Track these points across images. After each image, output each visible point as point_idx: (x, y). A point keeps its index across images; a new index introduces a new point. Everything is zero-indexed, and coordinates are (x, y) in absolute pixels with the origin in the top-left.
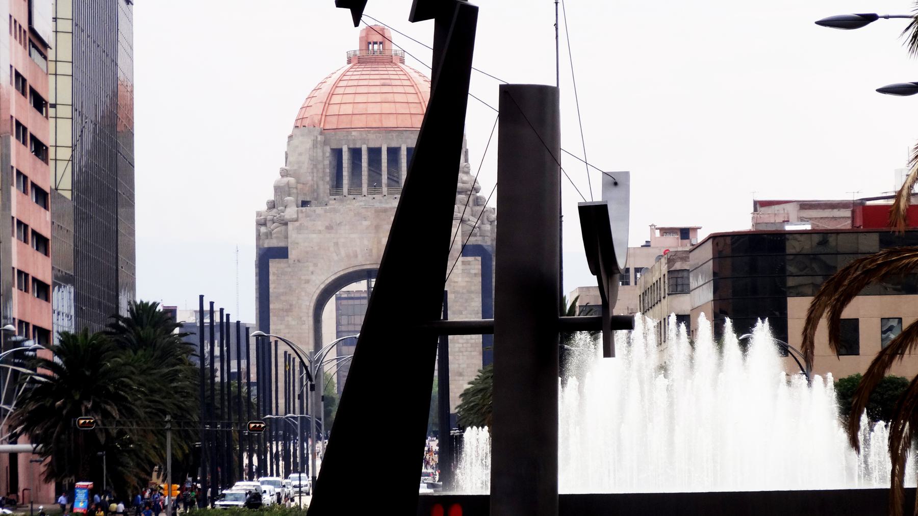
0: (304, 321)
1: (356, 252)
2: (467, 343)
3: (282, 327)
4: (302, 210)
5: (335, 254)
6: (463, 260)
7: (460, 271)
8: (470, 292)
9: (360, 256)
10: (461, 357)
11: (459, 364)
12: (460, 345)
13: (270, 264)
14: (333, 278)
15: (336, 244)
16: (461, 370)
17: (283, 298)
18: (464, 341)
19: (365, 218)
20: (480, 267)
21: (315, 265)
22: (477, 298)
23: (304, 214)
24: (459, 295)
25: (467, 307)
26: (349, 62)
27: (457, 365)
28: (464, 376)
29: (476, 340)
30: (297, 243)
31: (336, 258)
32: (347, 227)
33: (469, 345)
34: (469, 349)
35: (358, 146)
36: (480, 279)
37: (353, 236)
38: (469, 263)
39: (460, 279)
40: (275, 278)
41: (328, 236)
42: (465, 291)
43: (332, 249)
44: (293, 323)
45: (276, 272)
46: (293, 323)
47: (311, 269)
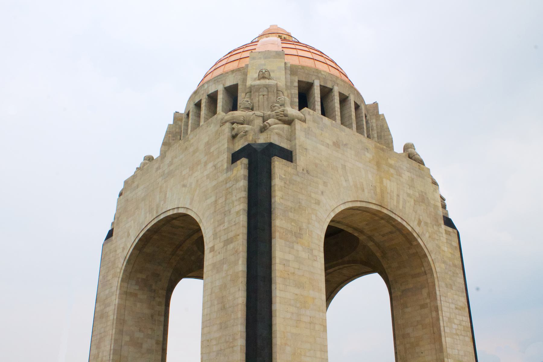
0: (316, 256)
2: (460, 325)
5: (342, 178)
7: (445, 241)
9: (366, 191)
14: (343, 208)
15: (344, 167)
17: (291, 215)
21: (325, 184)
30: (306, 149)
31: (344, 184)
35: (329, 85)
39: (446, 249)
40: (282, 184)
44: (304, 255)
45: (284, 177)
46: (304, 255)
47: (321, 187)
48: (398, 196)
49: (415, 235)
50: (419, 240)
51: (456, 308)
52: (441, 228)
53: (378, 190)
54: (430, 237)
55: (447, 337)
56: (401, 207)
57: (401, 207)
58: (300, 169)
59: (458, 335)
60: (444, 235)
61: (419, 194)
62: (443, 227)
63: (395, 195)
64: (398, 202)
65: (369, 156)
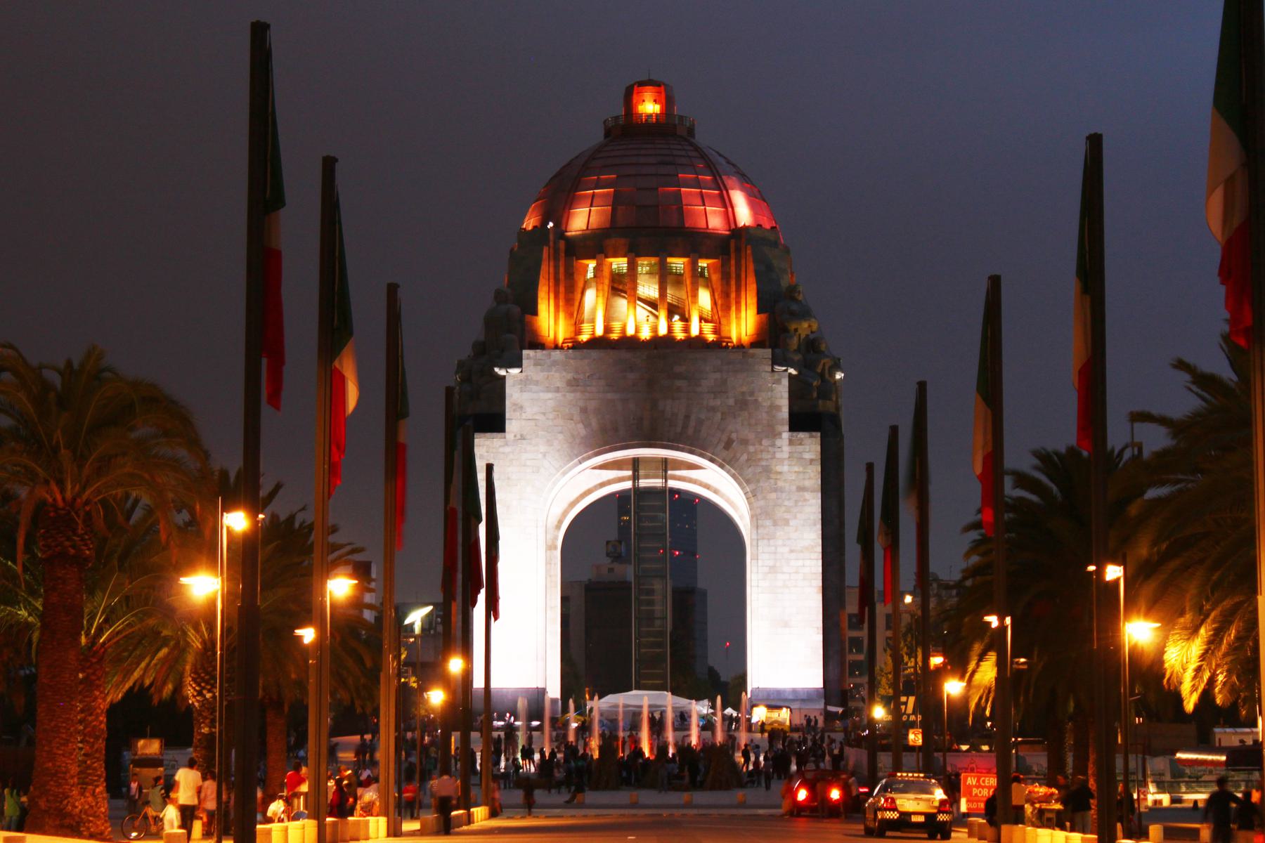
2: (797, 572)
4: (528, 355)
7: (786, 455)
13: (476, 441)
20: (819, 448)
22: (814, 498)
23: (532, 362)
24: (784, 495)
26: (608, 133)
30: (521, 407)
39: (785, 468)
42: (794, 488)
45: (486, 454)
51: (792, 551)
52: (781, 438)
54: (748, 460)
57: (690, 431)
60: (786, 448)
61: (736, 402)
62: (786, 435)
64: (685, 427)
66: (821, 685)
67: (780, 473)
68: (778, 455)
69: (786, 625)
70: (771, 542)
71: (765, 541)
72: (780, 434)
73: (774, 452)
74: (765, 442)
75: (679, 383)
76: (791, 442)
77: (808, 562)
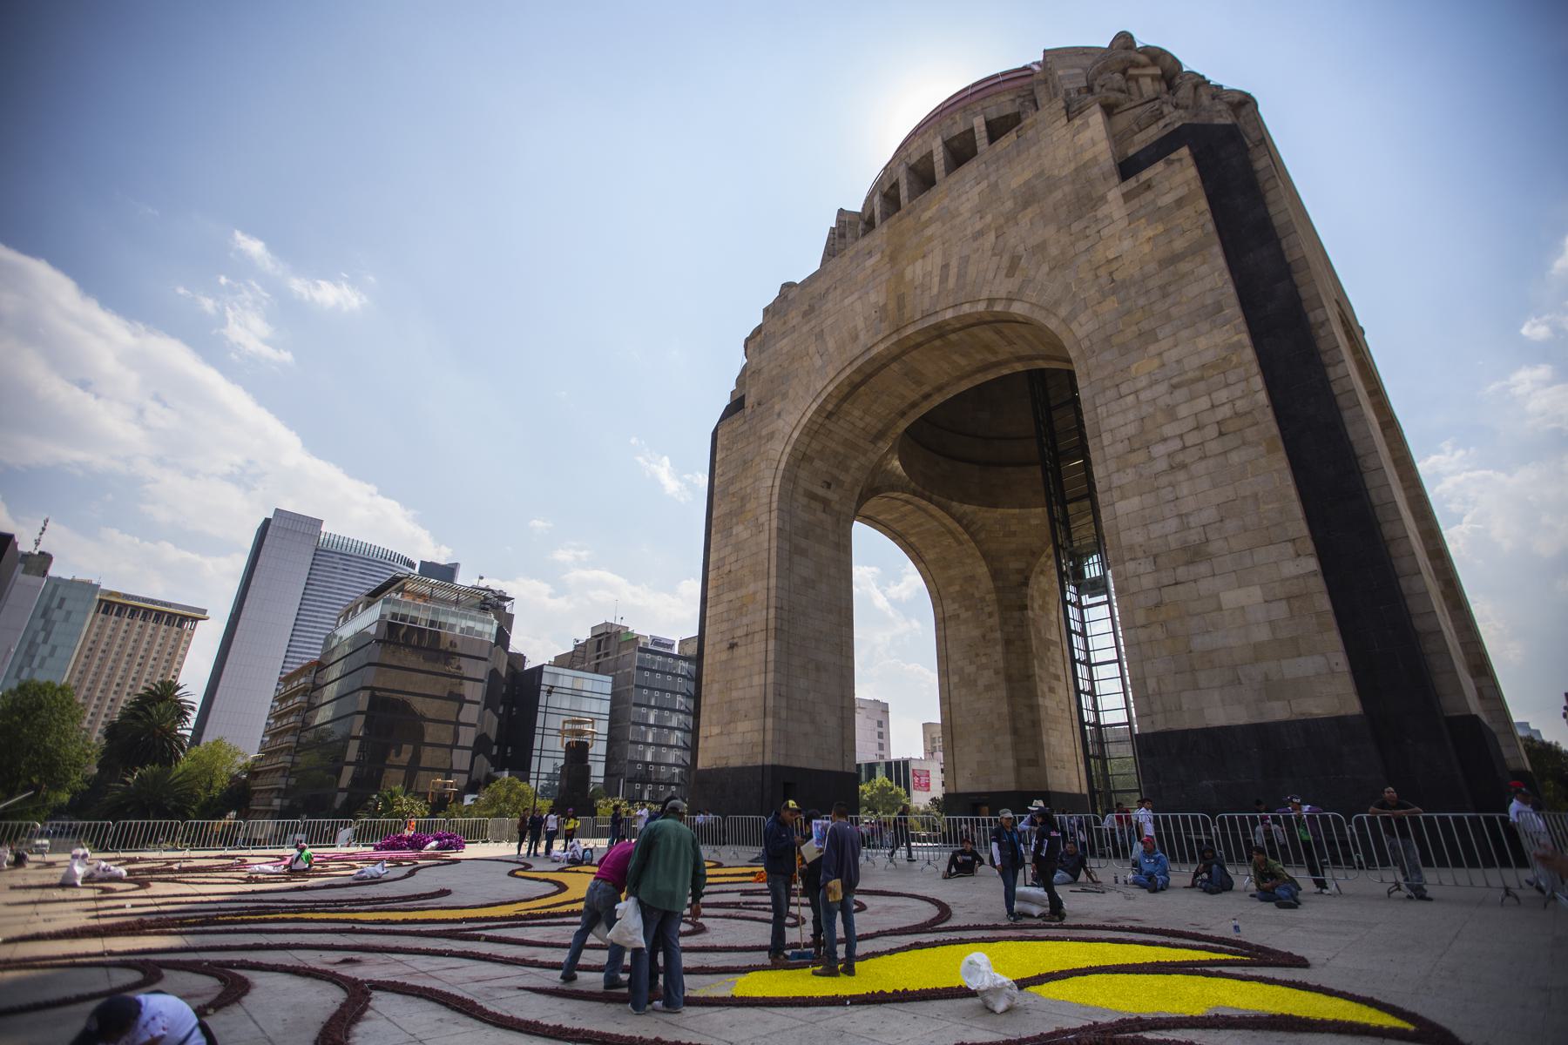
1: (856, 329)
2: (1199, 428)
3: (729, 549)
6: (1125, 190)
8: (1175, 259)
9: (863, 337)
10: (1185, 489)
11: (1180, 516)
12: (1177, 444)
16: (1194, 537)
18: (1191, 423)
19: (870, 254)
20: (1192, 172)
21: (784, 396)
22: (1204, 263)
24: (1133, 291)
25: (1174, 311)
27: (1173, 524)
28: (1209, 557)
29: (1239, 403)
31: (818, 362)
32: (839, 291)
33: (1212, 431)
34: (1214, 447)
36: (1203, 204)
37: (847, 302)
38: (1148, 186)
41: (805, 329)
42: (1152, 267)
43: (812, 349)
46: (745, 535)
47: (777, 408)
48: (946, 266)
49: (998, 308)
50: (1018, 309)
51: (1174, 387)
52: (1107, 202)
53: (892, 305)
54: (1051, 269)
55: (1123, 498)
56: (951, 282)
57: (951, 282)
58: (748, 411)
59: (1183, 466)
62: (1115, 194)
63: (937, 272)
65: (876, 257)
66: (1354, 707)
67: (1116, 258)
68: (1105, 232)
69: (1195, 554)
70: (1124, 389)
71: (1111, 394)
72: (1103, 199)
73: (1099, 232)
74: (1076, 227)
75: (928, 232)
76: (1127, 197)
77: (1222, 395)
